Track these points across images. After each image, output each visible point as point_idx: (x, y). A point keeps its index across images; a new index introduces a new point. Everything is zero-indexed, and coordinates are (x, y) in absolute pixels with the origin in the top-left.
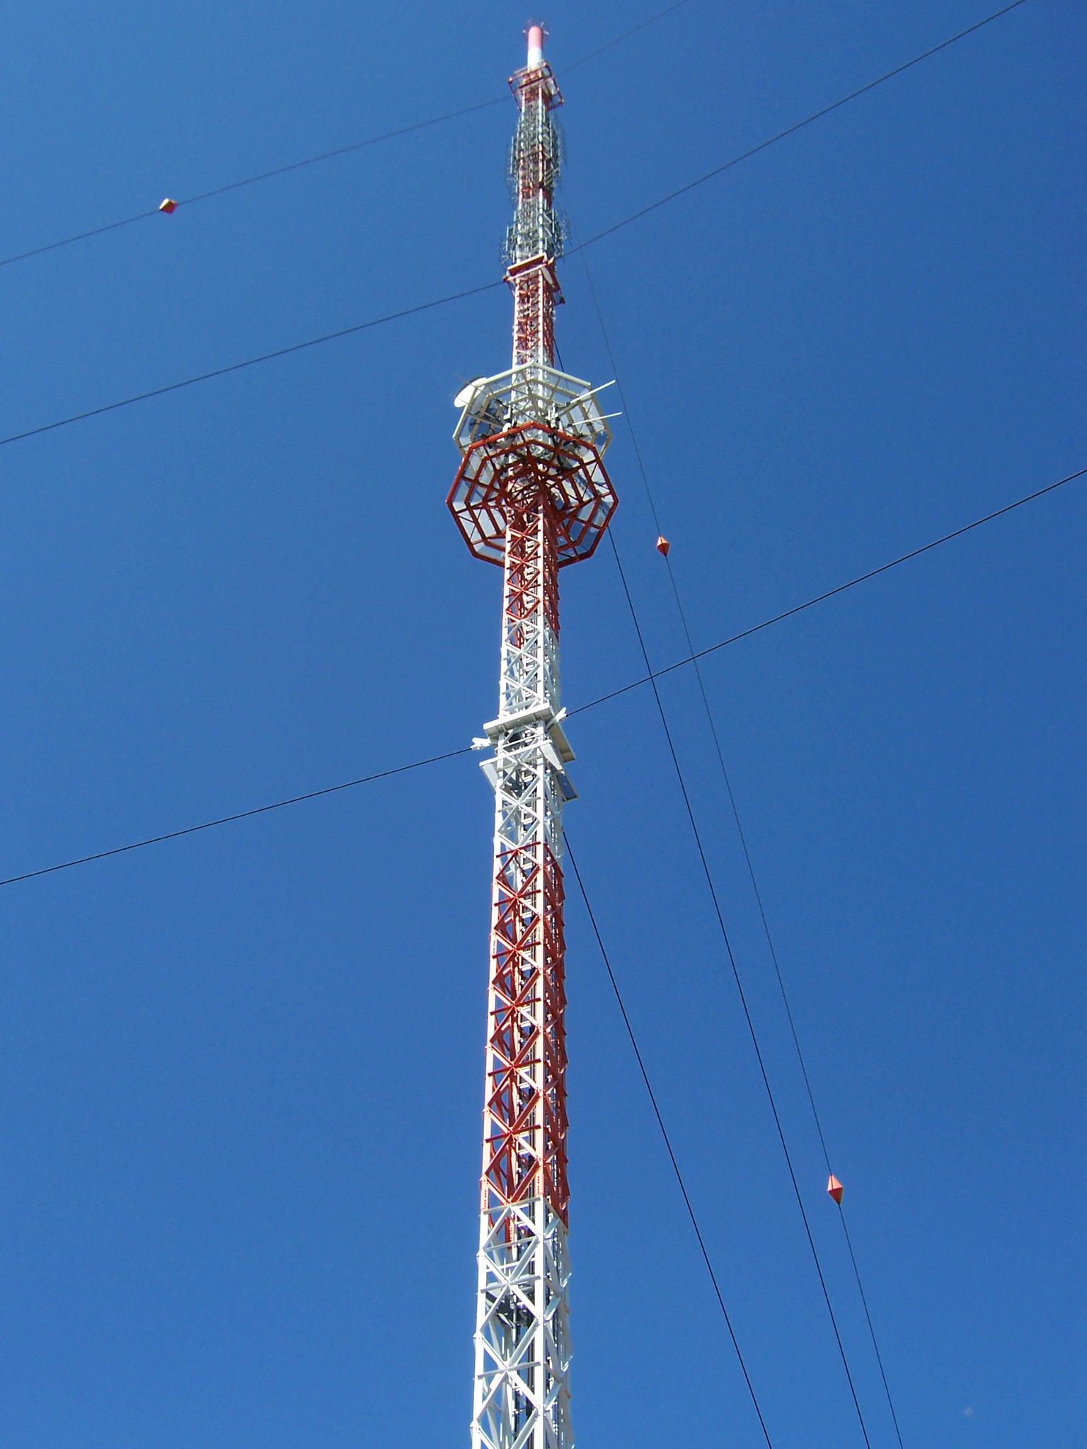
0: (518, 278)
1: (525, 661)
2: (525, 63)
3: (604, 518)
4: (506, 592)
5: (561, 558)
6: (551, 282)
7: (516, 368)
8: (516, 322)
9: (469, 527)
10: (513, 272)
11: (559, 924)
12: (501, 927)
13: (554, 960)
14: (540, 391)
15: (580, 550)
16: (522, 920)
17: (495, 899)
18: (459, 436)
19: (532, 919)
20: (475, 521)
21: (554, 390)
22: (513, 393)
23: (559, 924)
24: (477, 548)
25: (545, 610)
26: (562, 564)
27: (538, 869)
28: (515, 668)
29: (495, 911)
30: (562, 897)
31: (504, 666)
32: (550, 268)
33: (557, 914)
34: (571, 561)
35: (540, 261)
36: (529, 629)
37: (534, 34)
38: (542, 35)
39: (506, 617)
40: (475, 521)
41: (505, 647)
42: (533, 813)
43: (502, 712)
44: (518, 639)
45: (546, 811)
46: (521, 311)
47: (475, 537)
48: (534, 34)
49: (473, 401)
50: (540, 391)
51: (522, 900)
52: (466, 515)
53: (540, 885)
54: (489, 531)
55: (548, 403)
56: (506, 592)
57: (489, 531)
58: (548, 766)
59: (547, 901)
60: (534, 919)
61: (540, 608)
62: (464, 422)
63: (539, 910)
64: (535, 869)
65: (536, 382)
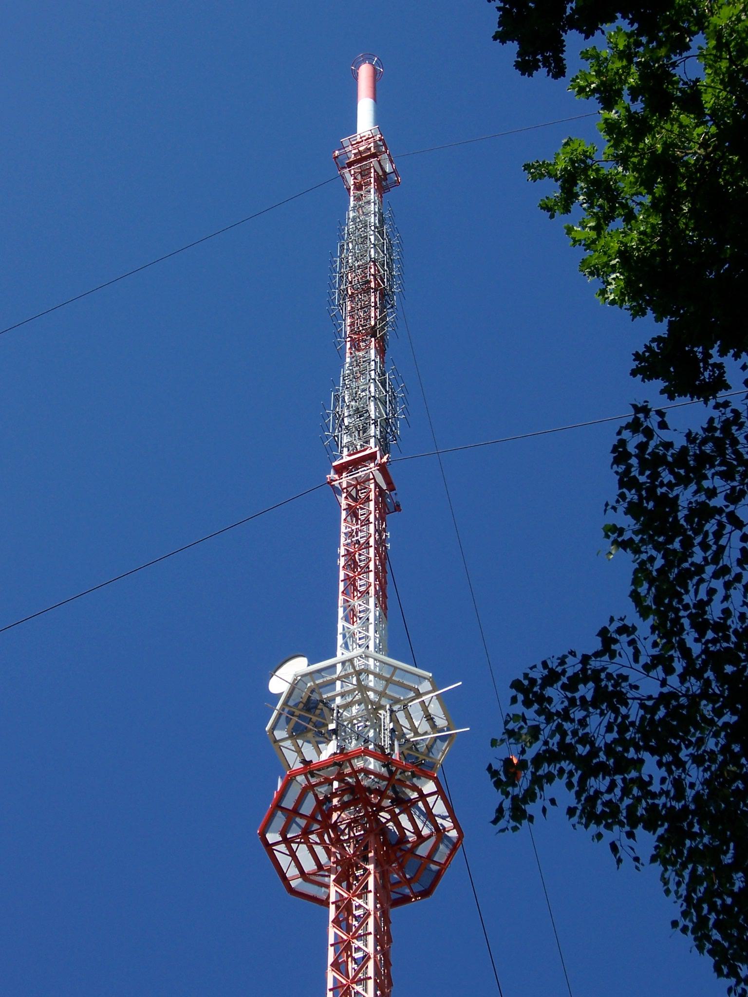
0: (345, 480)
1: (357, 636)
2: (355, 131)
3: (448, 852)
4: (342, 577)
5: (394, 896)
6: (381, 173)
7: (341, 654)
8: (342, 551)
9: (284, 861)
10: (339, 470)
11: (388, 964)
12: (336, 965)
13: (382, 947)
14: (371, 681)
15: (417, 887)
16: (354, 959)
17: (331, 940)
18: (273, 728)
19: (363, 957)
20: (293, 854)
21: (389, 681)
22: (338, 683)
23: (388, 964)
24: (293, 884)
25: (376, 592)
26: (397, 903)
27: (369, 958)
28: (350, 643)
29: (331, 950)
30: (390, 940)
31: (340, 640)
32: (382, 468)
33: (385, 954)
34: (406, 899)
35: (372, 457)
36: (361, 608)
37: (365, 72)
38: (375, 73)
39: (341, 598)
40: (293, 854)
41: (341, 624)
42: (364, 905)
43: (339, 651)
44: (351, 615)
45: (376, 632)
46: (350, 535)
47: (292, 871)
48: (365, 72)
49: (294, 686)
50: (371, 681)
51: (354, 986)
52: (282, 847)
53: (371, 972)
54: (309, 866)
55: (381, 694)
56: (342, 577)
57: (309, 866)
58: (377, 485)
59: (377, 942)
60: (366, 958)
61: (372, 590)
62: (280, 715)
63: (370, 949)
64: (366, 958)
65: (367, 672)
